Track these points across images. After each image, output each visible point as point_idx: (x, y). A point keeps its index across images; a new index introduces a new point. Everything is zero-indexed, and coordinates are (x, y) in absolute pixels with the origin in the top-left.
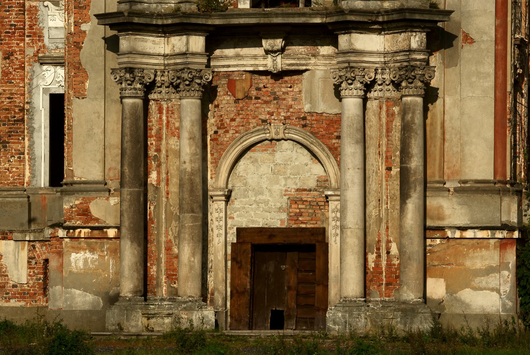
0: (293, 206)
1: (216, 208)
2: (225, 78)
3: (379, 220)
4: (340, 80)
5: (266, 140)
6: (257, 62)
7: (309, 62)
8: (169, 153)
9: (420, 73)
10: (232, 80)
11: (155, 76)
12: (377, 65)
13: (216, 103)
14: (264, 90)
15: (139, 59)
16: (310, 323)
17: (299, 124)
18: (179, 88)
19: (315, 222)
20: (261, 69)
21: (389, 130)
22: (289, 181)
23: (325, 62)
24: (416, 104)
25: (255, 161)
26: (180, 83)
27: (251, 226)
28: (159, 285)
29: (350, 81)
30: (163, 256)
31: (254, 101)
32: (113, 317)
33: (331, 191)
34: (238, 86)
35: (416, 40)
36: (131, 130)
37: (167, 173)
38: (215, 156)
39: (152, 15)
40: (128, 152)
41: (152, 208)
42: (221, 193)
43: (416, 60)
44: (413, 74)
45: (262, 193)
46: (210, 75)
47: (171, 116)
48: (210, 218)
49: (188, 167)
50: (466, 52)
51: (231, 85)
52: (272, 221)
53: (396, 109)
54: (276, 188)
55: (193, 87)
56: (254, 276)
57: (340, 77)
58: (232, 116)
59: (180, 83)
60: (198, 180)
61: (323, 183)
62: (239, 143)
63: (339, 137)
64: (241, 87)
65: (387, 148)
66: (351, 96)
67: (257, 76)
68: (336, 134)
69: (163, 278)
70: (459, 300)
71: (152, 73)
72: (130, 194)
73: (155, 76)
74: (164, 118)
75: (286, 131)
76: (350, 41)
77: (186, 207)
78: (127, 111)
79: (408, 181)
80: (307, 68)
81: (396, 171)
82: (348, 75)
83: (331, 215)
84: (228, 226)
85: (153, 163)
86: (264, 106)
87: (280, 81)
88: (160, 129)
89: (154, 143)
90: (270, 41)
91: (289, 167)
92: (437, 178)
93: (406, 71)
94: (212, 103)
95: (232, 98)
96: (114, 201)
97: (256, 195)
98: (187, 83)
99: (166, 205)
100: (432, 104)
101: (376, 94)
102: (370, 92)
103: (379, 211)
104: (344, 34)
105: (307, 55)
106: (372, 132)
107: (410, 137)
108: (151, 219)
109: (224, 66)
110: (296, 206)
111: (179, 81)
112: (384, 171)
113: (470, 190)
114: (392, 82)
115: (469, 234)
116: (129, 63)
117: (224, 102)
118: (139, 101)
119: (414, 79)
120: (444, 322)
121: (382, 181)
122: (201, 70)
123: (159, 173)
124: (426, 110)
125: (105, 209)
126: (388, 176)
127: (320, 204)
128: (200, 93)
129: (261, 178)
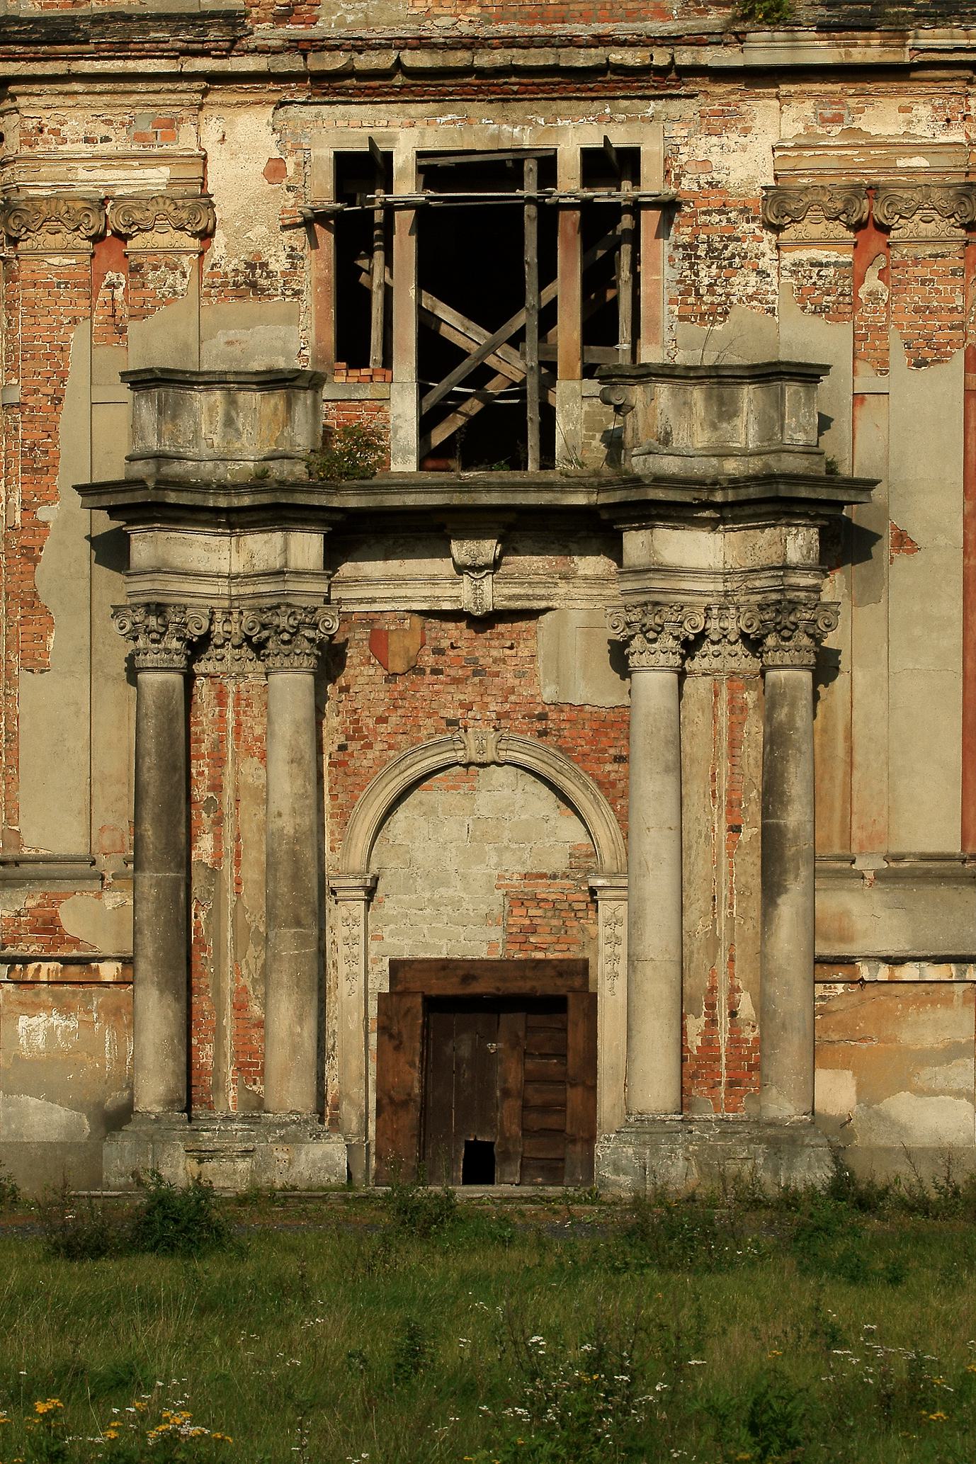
0: (516, 911)
1: (344, 916)
2: (363, 626)
3: (714, 942)
4: (629, 632)
5: (457, 764)
6: (438, 592)
7: (554, 591)
8: (241, 792)
9: (808, 616)
10: (380, 631)
11: (211, 621)
12: (710, 600)
13: (342, 681)
14: (451, 653)
15: (177, 585)
16: (554, 1171)
17: (530, 730)
18: (265, 648)
19: (565, 947)
20: (447, 606)
21: (733, 744)
22: (507, 856)
23: (589, 591)
24: (796, 686)
25: (430, 812)
26: (267, 639)
27: (422, 955)
28: (218, 1087)
29: (651, 635)
30: (228, 1022)
31: (429, 678)
32: (120, 1159)
33: (603, 877)
34: (395, 644)
35: (799, 543)
36: (158, 743)
37: (238, 839)
38: (339, 801)
39: (204, 487)
40: (152, 791)
41: (203, 915)
42: (357, 883)
43: (798, 588)
44: (792, 618)
45: (445, 883)
46: (334, 621)
47: (245, 712)
48: (329, 937)
49: (287, 825)
50: (901, 572)
51: (379, 644)
52: (470, 944)
53: (750, 697)
54: (478, 871)
55: (297, 646)
56: (432, 1064)
57: (628, 624)
58: (380, 710)
59: (267, 639)
60: (309, 854)
61: (584, 860)
62: (397, 771)
63: (620, 759)
64: (401, 648)
65: (731, 782)
66: (653, 668)
67: (435, 622)
68: (612, 751)
69: (229, 1070)
70: (883, 1118)
71: (203, 615)
72: (158, 884)
73: (211, 621)
74: (230, 715)
75: (501, 746)
76: (651, 544)
77: (282, 913)
78: (149, 699)
79: (781, 858)
80: (550, 604)
81: (751, 832)
82: (650, 621)
83: (603, 931)
84: (371, 956)
85: (204, 815)
86: (452, 689)
87: (488, 634)
88: (221, 740)
89: (206, 772)
90: (470, 545)
91: (508, 824)
92: (837, 850)
93: (778, 611)
94: (333, 680)
95: (381, 671)
96: (111, 900)
97: (432, 888)
98: (286, 637)
99: (235, 909)
100: (826, 686)
101: (705, 663)
102: (693, 658)
103: (714, 921)
104: (637, 529)
105: (549, 575)
106: (697, 747)
107: (784, 759)
108: (198, 941)
109: (360, 601)
110: (522, 911)
111: (265, 633)
112: (725, 835)
113: (908, 875)
114: (744, 636)
115: (909, 972)
116: (157, 592)
117: (361, 680)
118: (176, 679)
119: (793, 631)
120: (860, 1166)
121: (719, 855)
122: (316, 609)
123: (218, 839)
124: (816, 697)
125: (98, 918)
126: (733, 845)
127: (576, 906)
128: (313, 660)
129: (445, 849)
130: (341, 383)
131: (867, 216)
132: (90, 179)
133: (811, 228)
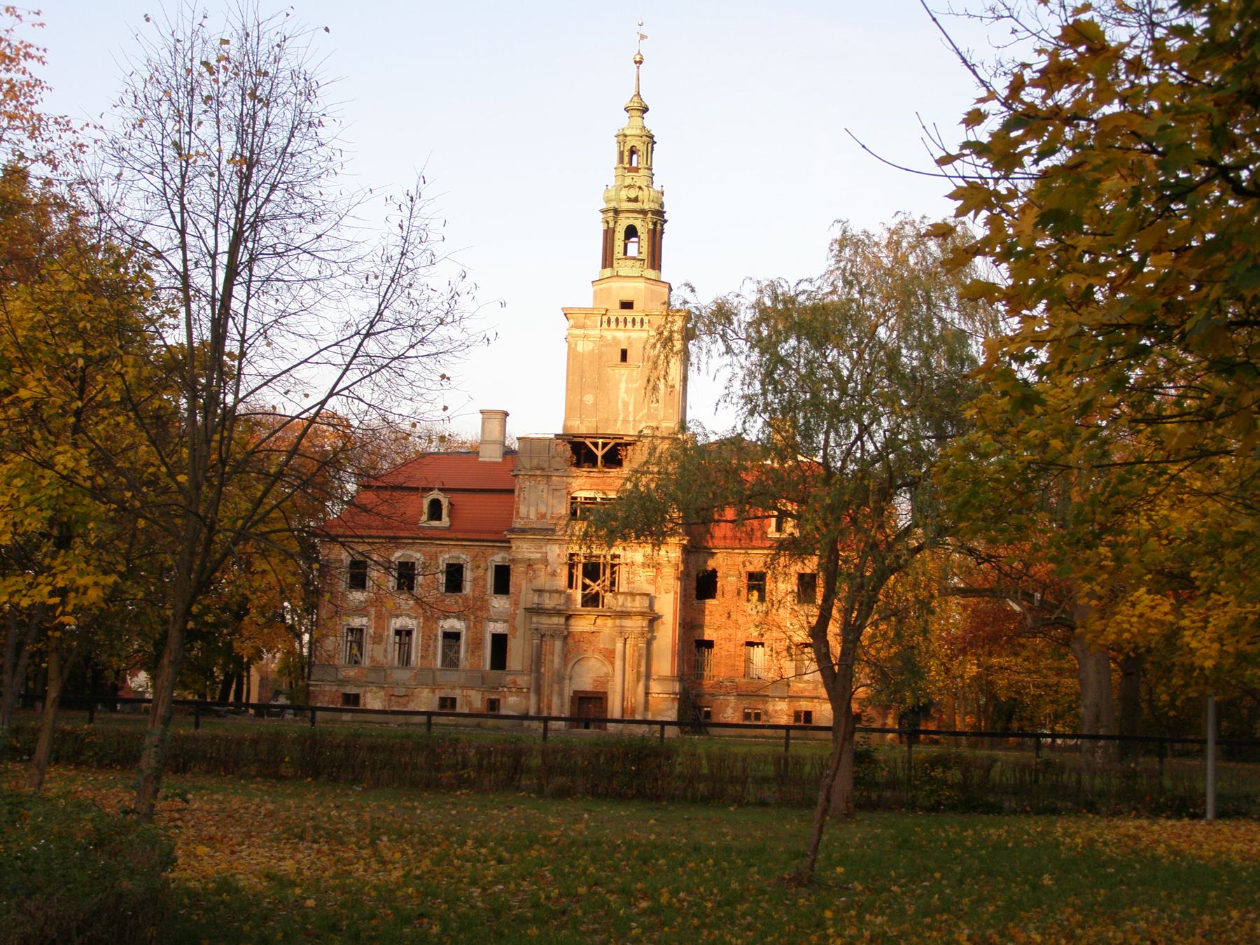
130: (569, 591)
132: (527, 556)
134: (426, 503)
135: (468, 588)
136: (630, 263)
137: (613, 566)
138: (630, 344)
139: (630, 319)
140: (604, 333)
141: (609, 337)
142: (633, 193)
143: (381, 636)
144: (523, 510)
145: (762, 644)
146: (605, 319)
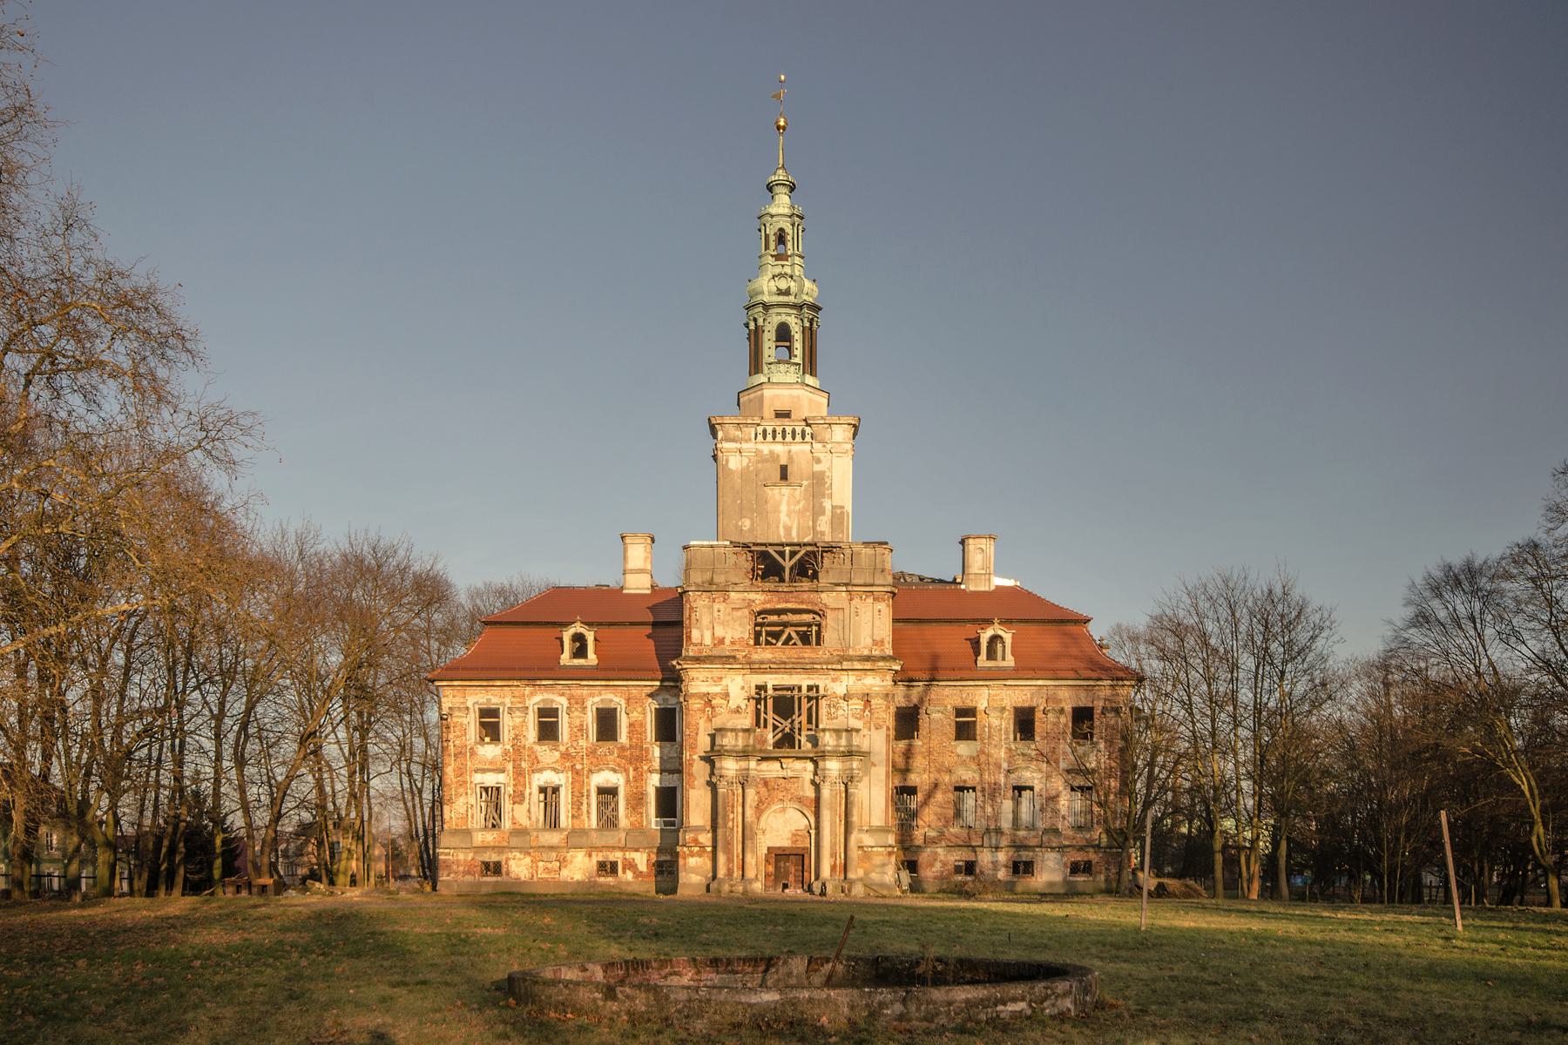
113: (872, 830)
131: (867, 699)
133: (854, 701)
134: (567, 636)
135: (623, 737)
136: (782, 367)
137: (810, 699)
138: (790, 458)
139: (789, 430)
140: (760, 446)
141: (766, 452)
142: (783, 284)
143: (522, 795)
144: (695, 634)
145: (974, 789)
146: (760, 429)
